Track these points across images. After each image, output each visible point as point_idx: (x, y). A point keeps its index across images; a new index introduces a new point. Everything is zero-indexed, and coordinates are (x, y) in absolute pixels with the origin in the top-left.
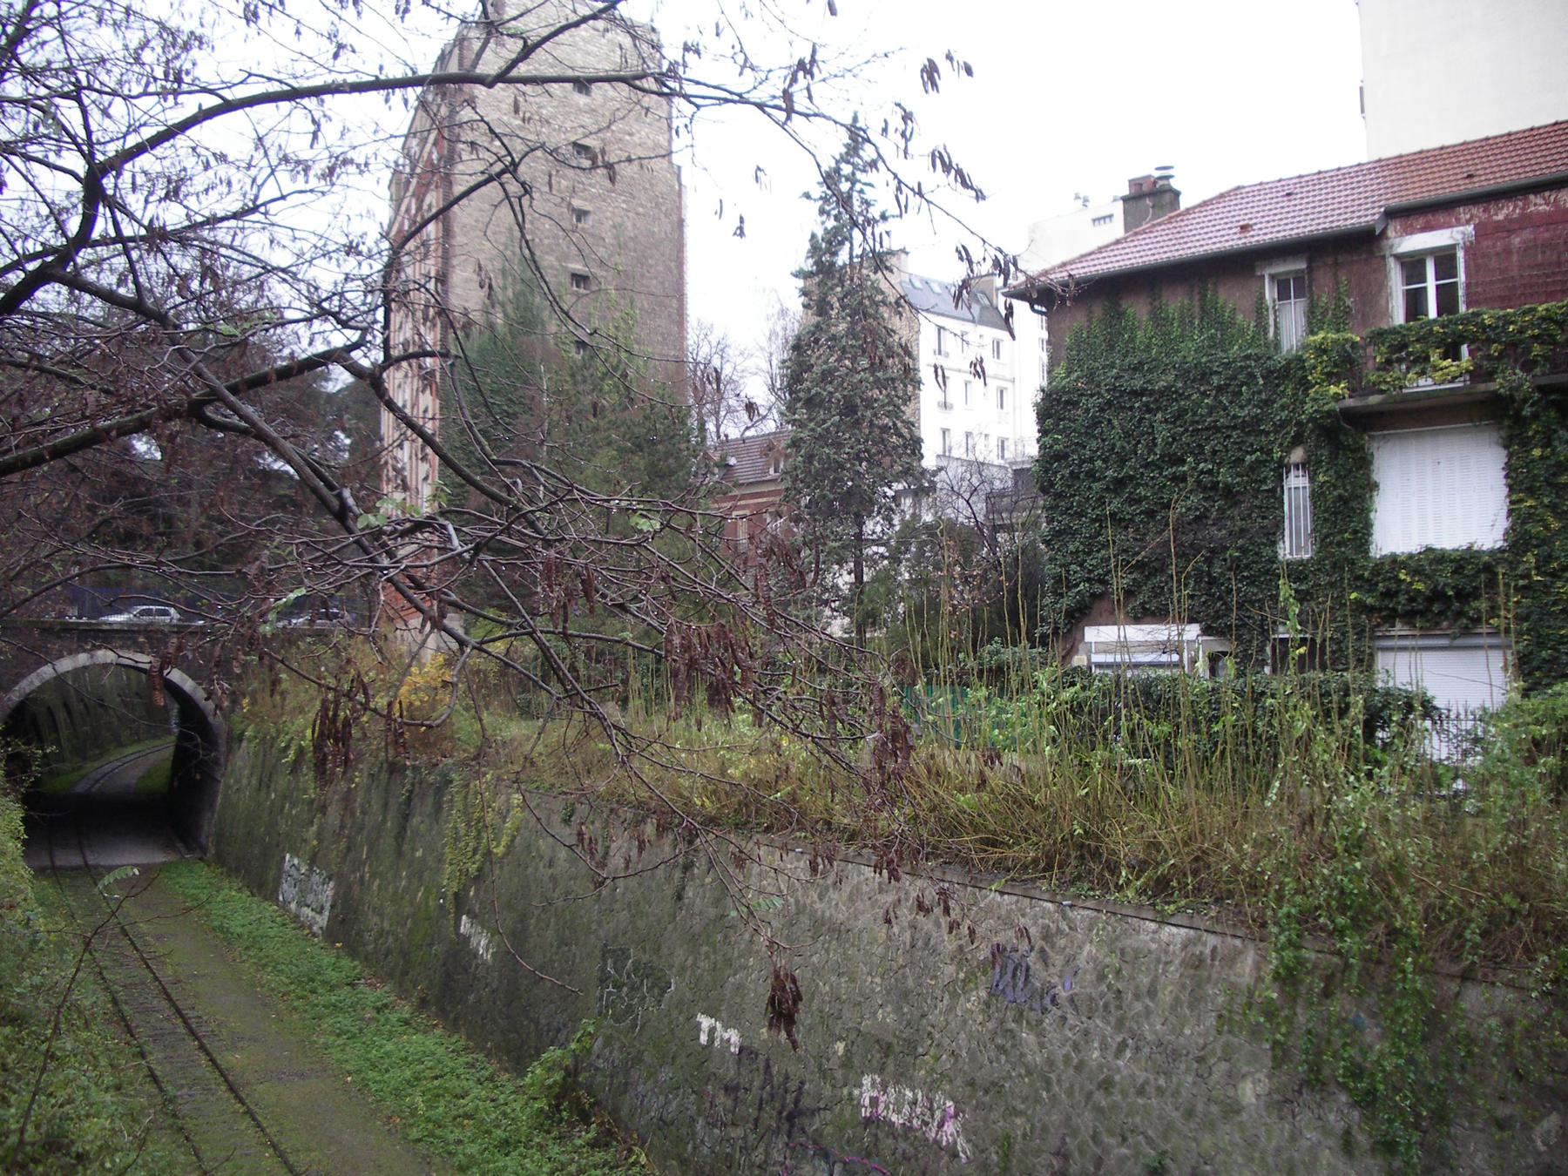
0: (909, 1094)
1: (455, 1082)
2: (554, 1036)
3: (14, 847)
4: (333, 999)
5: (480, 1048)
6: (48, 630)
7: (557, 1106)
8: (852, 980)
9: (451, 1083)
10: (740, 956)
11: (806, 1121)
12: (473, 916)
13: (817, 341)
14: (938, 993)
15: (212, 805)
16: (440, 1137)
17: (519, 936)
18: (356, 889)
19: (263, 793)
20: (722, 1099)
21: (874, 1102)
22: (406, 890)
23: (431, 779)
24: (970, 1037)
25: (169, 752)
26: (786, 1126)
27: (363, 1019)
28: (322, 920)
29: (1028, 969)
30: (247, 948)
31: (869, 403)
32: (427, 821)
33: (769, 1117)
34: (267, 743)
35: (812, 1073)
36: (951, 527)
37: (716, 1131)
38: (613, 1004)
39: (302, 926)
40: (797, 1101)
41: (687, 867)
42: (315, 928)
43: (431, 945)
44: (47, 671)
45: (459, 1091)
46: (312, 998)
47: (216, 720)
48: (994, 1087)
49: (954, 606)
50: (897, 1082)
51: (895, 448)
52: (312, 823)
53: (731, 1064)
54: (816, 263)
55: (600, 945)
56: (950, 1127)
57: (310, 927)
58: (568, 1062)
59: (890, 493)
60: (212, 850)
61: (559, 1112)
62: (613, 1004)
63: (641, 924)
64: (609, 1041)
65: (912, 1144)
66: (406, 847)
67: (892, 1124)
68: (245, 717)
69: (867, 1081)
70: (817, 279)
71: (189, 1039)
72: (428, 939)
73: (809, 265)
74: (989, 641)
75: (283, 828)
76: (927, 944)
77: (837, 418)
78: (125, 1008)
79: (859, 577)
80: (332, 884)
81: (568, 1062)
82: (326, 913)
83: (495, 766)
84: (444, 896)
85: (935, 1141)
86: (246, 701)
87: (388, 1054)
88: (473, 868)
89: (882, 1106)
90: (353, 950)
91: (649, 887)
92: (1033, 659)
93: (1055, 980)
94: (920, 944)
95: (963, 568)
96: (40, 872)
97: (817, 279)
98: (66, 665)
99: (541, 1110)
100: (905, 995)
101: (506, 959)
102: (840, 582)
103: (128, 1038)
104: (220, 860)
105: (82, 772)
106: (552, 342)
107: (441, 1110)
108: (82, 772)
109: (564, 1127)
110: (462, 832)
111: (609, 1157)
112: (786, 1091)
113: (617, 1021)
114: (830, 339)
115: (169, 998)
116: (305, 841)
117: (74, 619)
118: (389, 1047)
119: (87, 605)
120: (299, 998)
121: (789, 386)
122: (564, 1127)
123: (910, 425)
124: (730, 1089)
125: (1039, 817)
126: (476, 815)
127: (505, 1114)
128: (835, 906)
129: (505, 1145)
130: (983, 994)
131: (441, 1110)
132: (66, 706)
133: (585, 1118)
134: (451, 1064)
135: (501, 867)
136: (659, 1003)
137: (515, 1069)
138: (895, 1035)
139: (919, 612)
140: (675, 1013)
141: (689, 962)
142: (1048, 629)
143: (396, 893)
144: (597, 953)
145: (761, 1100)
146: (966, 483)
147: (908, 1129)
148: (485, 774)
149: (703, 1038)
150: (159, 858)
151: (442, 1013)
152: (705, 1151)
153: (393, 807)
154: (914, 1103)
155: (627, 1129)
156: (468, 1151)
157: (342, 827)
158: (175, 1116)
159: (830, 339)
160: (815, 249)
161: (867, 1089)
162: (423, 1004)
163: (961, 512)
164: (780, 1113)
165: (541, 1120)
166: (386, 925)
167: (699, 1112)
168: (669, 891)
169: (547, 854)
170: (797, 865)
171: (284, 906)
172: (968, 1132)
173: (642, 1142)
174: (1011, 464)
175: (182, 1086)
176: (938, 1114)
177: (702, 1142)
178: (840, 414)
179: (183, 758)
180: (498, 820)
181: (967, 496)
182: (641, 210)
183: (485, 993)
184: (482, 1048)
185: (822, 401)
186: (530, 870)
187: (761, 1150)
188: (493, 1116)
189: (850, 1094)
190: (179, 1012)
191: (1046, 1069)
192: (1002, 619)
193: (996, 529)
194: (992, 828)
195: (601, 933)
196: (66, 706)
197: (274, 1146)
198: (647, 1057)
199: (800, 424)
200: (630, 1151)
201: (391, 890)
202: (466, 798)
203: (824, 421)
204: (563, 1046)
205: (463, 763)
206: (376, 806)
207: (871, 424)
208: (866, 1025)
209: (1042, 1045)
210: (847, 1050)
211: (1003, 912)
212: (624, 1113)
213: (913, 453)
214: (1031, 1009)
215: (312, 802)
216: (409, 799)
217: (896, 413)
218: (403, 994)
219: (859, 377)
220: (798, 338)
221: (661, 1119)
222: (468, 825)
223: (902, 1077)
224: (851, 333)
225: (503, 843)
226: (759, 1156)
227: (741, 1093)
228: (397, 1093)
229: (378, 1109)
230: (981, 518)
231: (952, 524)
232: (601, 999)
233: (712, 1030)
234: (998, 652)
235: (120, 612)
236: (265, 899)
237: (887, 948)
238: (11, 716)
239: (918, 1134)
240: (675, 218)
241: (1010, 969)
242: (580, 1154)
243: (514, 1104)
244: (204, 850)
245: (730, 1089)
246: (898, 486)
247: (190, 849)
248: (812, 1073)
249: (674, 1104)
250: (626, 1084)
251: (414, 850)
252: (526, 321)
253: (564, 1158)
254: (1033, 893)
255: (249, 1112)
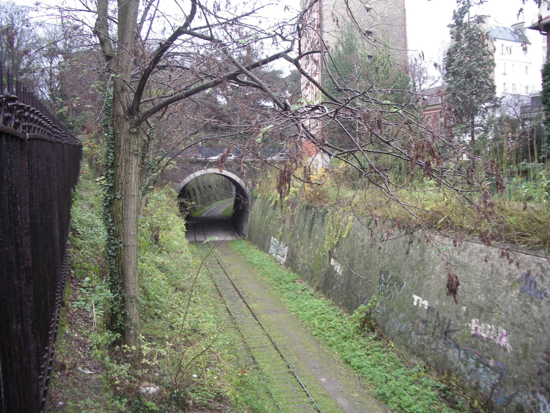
0: (489, 326)
1: (329, 316)
2: (363, 301)
3: (183, 234)
4: (287, 286)
5: (337, 304)
6: (192, 162)
7: (363, 326)
8: (469, 284)
9: (327, 316)
10: (429, 275)
11: (451, 334)
12: (335, 259)
13: (456, 51)
14: (501, 290)
15: (247, 221)
16: (323, 335)
17: (352, 265)
18: (295, 249)
19: (264, 216)
20: (421, 325)
21: (476, 329)
22: (312, 249)
23: (321, 211)
24: (513, 306)
25: (232, 203)
26: (444, 336)
27: (297, 293)
28: (284, 260)
29: (536, 283)
30: (259, 269)
31: (477, 73)
32: (319, 226)
33: (438, 332)
34: (265, 199)
35: (454, 317)
36: (508, 119)
37: (419, 336)
38: (383, 291)
39: (277, 262)
40: (448, 327)
41: (411, 242)
42: (282, 262)
43: (321, 268)
44: (192, 176)
45: (330, 319)
46: (280, 286)
47: (247, 191)
48: (522, 326)
49: (509, 148)
50: (485, 322)
51: (486, 89)
52: (280, 226)
53: (425, 313)
54: (456, 22)
55: (379, 269)
56: (504, 340)
57: (280, 262)
58: (367, 310)
59: (484, 107)
60: (247, 236)
61: (364, 327)
62: (383, 291)
63: (394, 262)
64: (382, 303)
65: (490, 345)
66: (312, 235)
67: (482, 337)
68: (257, 190)
69: (474, 321)
70: (456, 27)
71: (240, 299)
72: (320, 267)
73: (453, 22)
74: (522, 160)
75: (271, 228)
76: (497, 272)
77: (464, 79)
78: (219, 288)
79: (473, 138)
80: (287, 247)
81: (367, 310)
82: (285, 257)
83: (343, 206)
84: (325, 252)
85: (499, 344)
86: (258, 185)
87: (306, 306)
88: (335, 242)
89: (479, 330)
90: (294, 270)
91: (397, 250)
92: (539, 167)
93: (546, 287)
94: (495, 272)
95: (512, 134)
96: (191, 243)
97: (456, 27)
98: (198, 174)
99: (358, 326)
100: (489, 290)
101: (348, 273)
102: (465, 139)
103: (220, 297)
104: (250, 239)
105: (204, 210)
106: (360, 56)
107: (323, 325)
108: (204, 210)
109: (366, 333)
110: (332, 230)
111: (381, 344)
112: (444, 323)
113: (385, 296)
114: (461, 50)
115: (233, 285)
116: (278, 233)
117: (200, 159)
118: (306, 303)
119: (204, 153)
120: (276, 286)
121: (446, 68)
122: (366, 333)
123: (492, 80)
124: (424, 322)
125: (541, 226)
126: (336, 224)
127: (345, 328)
128: (463, 258)
129: (345, 338)
130: (518, 291)
131: (323, 325)
132: (199, 188)
133: (373, 330)
134: (327, 310)
135: (345, 242)
136: (400, 290)
137: (349, 312)
138: (485, 305)
139: (496, 150)
140: (405, 294)
141: (411, 276)
142: (544, 156)
143: (309, 251)
144: (378, 272)
145: (435, 326)
146: (513, 102)
147: (488, 339)
148: (339, 209)
149: (415, 303)
150: (229, 238)
151: (324, 292)
152: (415, 343)
153: (308, 221)
154: (491, 330)
155: (387, 335)
156: (332, 339)
157: (291, 228)
158: (235, 324)
159: (461, 50)
160: (455, 16)
161: (474, 324)
162: (318, 289)
163: (512, 113)
164: (442, 331)
165: (358, 330)
166: (305, 261)
167: (413, 330)
168: (404, 251)
169: (361, 237)
170: (448, 242)
171: (271, 255)
172: (511, 342)
173: (393, 339)
174: (530, 95)
175: (238, 314)
176: (500, 334)
177: (414, 340)
178: (465, 78)
179: (237, 203)
180: (344, 225)
181: (513, 106)
182: (390, 6)
183: (339, 285)
184: (338, 305)
185: (459, 73)
186: (355, 243)
187: (435, 344)
188: (341, 328)
189: (467, 325)
190: (236, 290)
191: (542, 320)
192: (527, 152)
193: (525, 119)
194: (522, 230)
195: (380, 265)
196: (199, 188)
197: (268, 335)
198: (395, 309)
199: (450, 82)
200: (388, 342)
201: (307, 249)
202: (333, 218)
203: (460, 81)
204: (365, 304)
205: (332, 206)
206: (302, 221)
207: (477, 81)
208: (474, 301)
209: (540, 311)
210: (467, 310)
211: (526, 261)
212: (386, 329)
213: (493, 92)
214: (537, 298)
215: (280, 219)
216: (313, 218)
217: (486, 77)
218: (311, 285)
219: (472, 63)
220: (449, 50)
221: (399, 331)
222: (334, 227)
223: (487, 320)
224: (469, 47)
225: (346, 233)
226: (433, 346)
227: (428, 324)
228: (309, 319)
229: (302, 324)
230: (519, 115)
231: (508, 117)
232: (379, 288)
233: (418, 301)
234: (525, 165)
235: (215, 155)
236: (265, 252)
237: (483, 273)
238: (181, 191)
239: (492, 341)
240: (402, 9)
241: (529, 282)
242: (371, 342)
243: (349, 324)
244: (245, 236)
245: (424, 322)
246: (487, 104)
247: (240, 235)
248: (454, 317)
249: (404, 326)
250: (387, 319)
251: (315, 236)
252: (350, 49)
253: (365, 343)
254: (538, 254)
255: (259, 324)
